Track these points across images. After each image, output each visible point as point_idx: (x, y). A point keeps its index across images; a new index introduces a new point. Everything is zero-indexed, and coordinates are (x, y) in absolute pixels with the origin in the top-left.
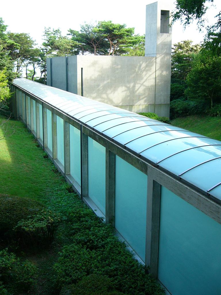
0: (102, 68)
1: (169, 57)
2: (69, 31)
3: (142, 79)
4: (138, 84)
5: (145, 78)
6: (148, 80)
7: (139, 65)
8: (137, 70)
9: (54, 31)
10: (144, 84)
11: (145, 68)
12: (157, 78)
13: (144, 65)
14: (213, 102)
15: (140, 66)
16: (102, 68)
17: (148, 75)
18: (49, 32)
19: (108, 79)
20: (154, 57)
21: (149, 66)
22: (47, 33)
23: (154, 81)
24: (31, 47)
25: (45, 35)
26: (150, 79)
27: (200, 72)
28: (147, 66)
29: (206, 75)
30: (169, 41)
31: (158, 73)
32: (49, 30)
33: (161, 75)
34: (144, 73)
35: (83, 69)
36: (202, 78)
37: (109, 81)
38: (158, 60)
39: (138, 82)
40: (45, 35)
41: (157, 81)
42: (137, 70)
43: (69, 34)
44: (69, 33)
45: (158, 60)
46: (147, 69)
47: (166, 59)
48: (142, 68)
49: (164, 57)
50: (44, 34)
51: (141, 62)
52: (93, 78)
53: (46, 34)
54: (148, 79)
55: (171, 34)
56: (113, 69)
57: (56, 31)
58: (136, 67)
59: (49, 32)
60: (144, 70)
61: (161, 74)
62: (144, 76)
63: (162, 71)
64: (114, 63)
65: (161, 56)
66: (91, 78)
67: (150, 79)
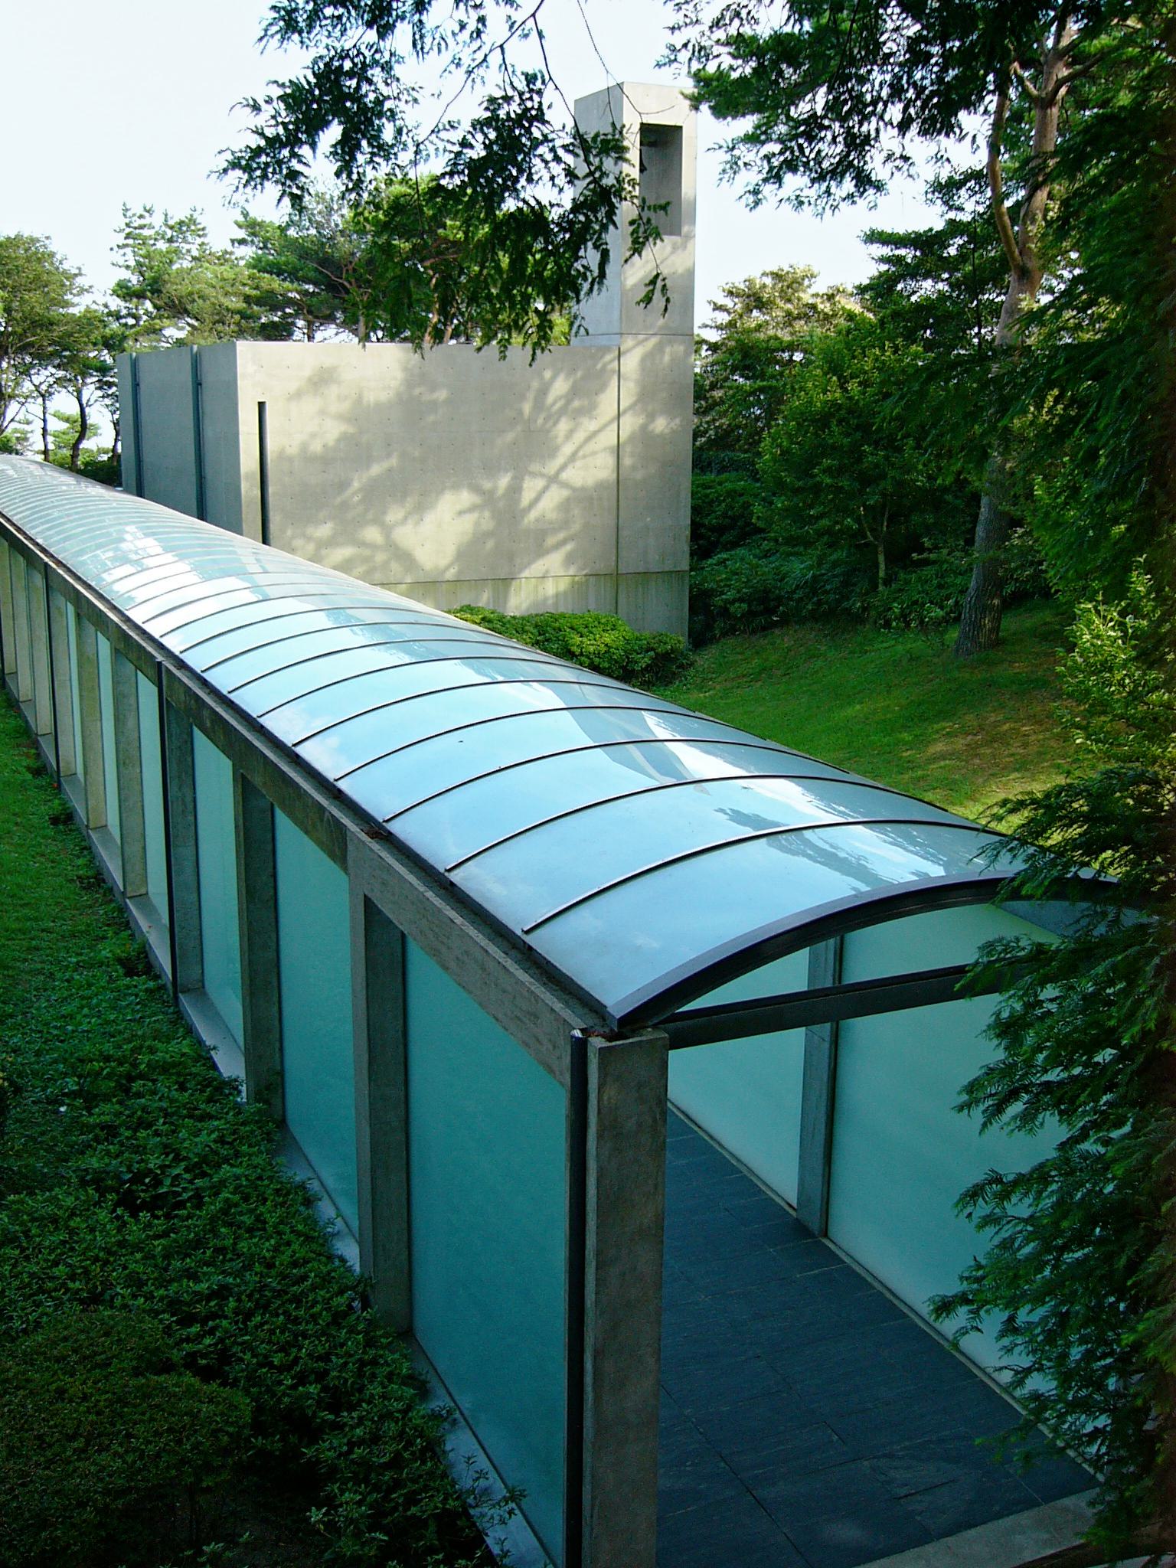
0: (359, 400)
1: (682, 348)
2: (240, 227)
3: (553, 452)
4: (534, 475)
5: (567, 450)
6: (584, 457)
7: (535, 384)
8: (527, 408)
9: (171, 222)
10: (564, 476)
11: (569, 402)
12: (627, 450)
13: (560, 386)
14: (887, 560)
15: (544, 391)
16: (359, 400)
17: (580, 436)
18: (146, 232)
19: (389, 455)
20: (607, 349)
21: (585, 392)
22: (133, 235)
23: (611, 461)
24: (67, 304)
25: (126, 246)
26: (594, 453)
27: (823, 420)
28: (574, 392)
29: (848, 435)
30: (680, 271)
31: (630, 424)
32: (142, 222)
33: (644, 436)
34: (563, 426)
35: (268, 407)
36: (834, 448)
37: (394, 461)
38: (631, 363)
39: (535, 467)
40: (126, 246)
41: (627, 461)
42: (527, 408)
43: (242, 242)
44: (242, 234)
45: (631, 363)
46: (576, 404)
47: (667, 358)
48: (554, 403)
49: (659, 348)
50: (122, 242)
51: (548, 374)
52: (317, 447)
53: (130, 241)
54: (581, 453)
55: (690, 237)
56: (410, 407)
57: (181, 223)
58: (522, 397)
59: (146, 232)
60: (563, 412)
61: (644, 428)
62: (560, 440)
63: (651, 417)
64: (415, 379)
65: (639, 343)
66: (304, 448)
67: (594, 453)
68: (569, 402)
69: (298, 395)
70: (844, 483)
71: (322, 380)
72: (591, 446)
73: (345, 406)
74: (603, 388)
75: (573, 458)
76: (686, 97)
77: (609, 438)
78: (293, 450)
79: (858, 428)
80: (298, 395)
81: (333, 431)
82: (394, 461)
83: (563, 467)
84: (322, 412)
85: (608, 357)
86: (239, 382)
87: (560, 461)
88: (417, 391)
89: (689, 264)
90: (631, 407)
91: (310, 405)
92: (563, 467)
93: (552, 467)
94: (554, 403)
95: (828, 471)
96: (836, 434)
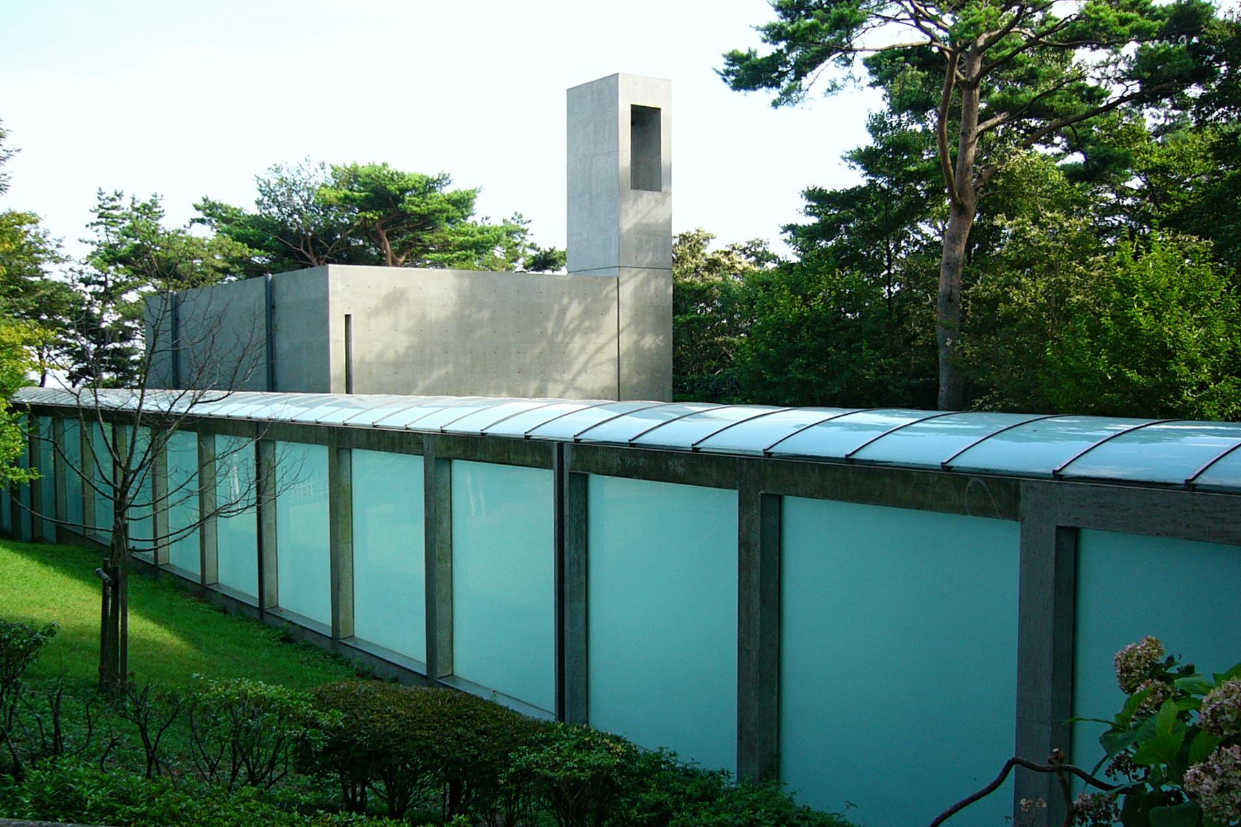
0: (424, 316)
1: (662, 282)
3: (570, 363)
4: (556, 381)
5: (583, 358)
6: (594, 366)
7: (556, 307)
8: (550, 327)
10: (579, 382)
11: (582, 322)
12: (624, 363)
13: (575, 310)
15: (563, 311)
16: (424, 316)
17: (591, 348)
20: (607, 281)
21: (592, 313)
23: (612, 369)
26: (602, 363)
27: (794, 329)
28: (586, 314)
29: (814, 340)
30: (661, 220)
31: (627, 340)
33: (638, 350)
34: (578, 342)
35: (353, 319)
36: (803, 350)
37: (450, 368)
38: (627, 291)
39: (556, 376)
41: (624, 371)
42: (550, 327)
45: (627, 291)
46: (587, 324)
47: (652, 289)
48: (571, 323)
49: (646, 282)
51: (565, 300)
52: (390, 355)
54: (590, 365)
55: (668, 194)
56: (463, 325)
58: (547, 319)
60: (577, 329)
61: (637, 343)
62: (575, 352)
63: (642, 334)
64: (468, 300)
65: (635, 276)
66: (380, 355)
67: (602, 363)
68: (582, 322)
69: (376, 312)
70: (813, 378)
71: (394, 300)
72: (598, 359)
73: (412, 323)
74: (604, 312)
75: (584, 369)
76: (718, 72)
77: (611, 351)
78: (370, 357)
79: (821, 334)
80: (376, 312)
81: (402, 343)
82: (450, 368)
83: (579, 373)
84: (395, 327)
85: (610, 288)
86: (331, 298)
87: (576, 367)
88: (467, 312)
89: (667, 216)
90: (628, 326)
91: (386, 321)
92: (579, 373)
93: (568, 377)
94: (571, 323)
95: (800, 367)
96: (806, 339)
